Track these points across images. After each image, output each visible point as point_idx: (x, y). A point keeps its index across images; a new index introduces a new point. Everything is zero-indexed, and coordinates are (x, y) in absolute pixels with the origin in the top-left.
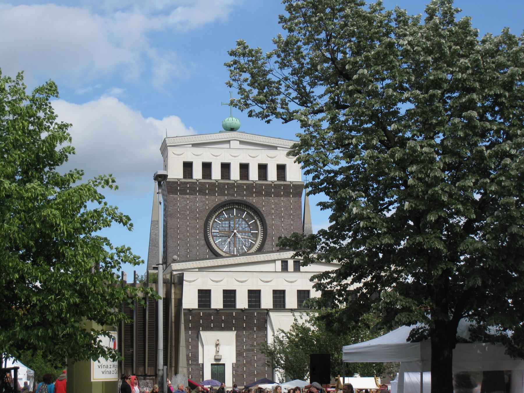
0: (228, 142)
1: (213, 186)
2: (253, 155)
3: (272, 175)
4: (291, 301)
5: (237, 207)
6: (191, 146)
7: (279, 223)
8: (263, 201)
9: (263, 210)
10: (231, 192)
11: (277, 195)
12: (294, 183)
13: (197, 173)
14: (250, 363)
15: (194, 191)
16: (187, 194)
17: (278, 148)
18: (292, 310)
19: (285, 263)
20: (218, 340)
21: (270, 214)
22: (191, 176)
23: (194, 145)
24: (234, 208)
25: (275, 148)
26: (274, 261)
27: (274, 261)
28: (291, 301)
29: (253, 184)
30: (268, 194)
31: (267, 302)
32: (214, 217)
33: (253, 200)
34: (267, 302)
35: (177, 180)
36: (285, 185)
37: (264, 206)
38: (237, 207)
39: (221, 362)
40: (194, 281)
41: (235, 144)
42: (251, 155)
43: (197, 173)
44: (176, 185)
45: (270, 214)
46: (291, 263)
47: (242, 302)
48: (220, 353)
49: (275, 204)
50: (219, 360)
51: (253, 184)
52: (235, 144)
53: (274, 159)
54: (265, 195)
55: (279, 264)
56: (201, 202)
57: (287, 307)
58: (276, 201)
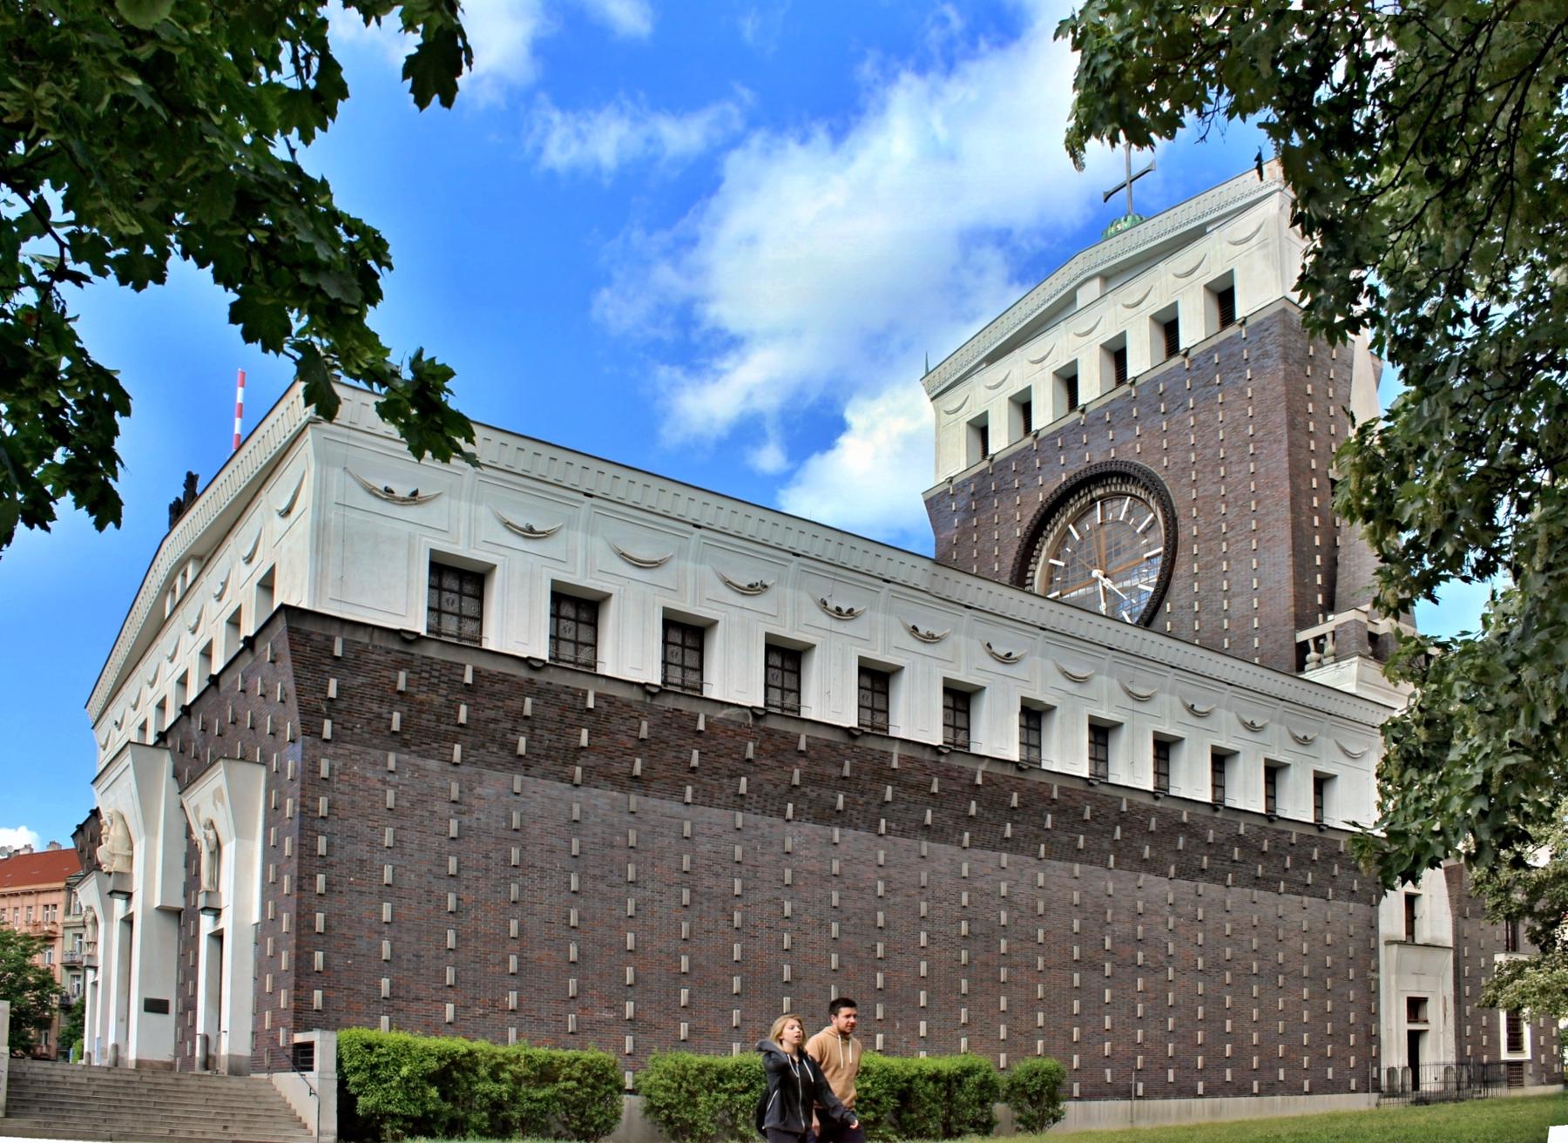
9: (1159, 466)
33: (1129, 448)
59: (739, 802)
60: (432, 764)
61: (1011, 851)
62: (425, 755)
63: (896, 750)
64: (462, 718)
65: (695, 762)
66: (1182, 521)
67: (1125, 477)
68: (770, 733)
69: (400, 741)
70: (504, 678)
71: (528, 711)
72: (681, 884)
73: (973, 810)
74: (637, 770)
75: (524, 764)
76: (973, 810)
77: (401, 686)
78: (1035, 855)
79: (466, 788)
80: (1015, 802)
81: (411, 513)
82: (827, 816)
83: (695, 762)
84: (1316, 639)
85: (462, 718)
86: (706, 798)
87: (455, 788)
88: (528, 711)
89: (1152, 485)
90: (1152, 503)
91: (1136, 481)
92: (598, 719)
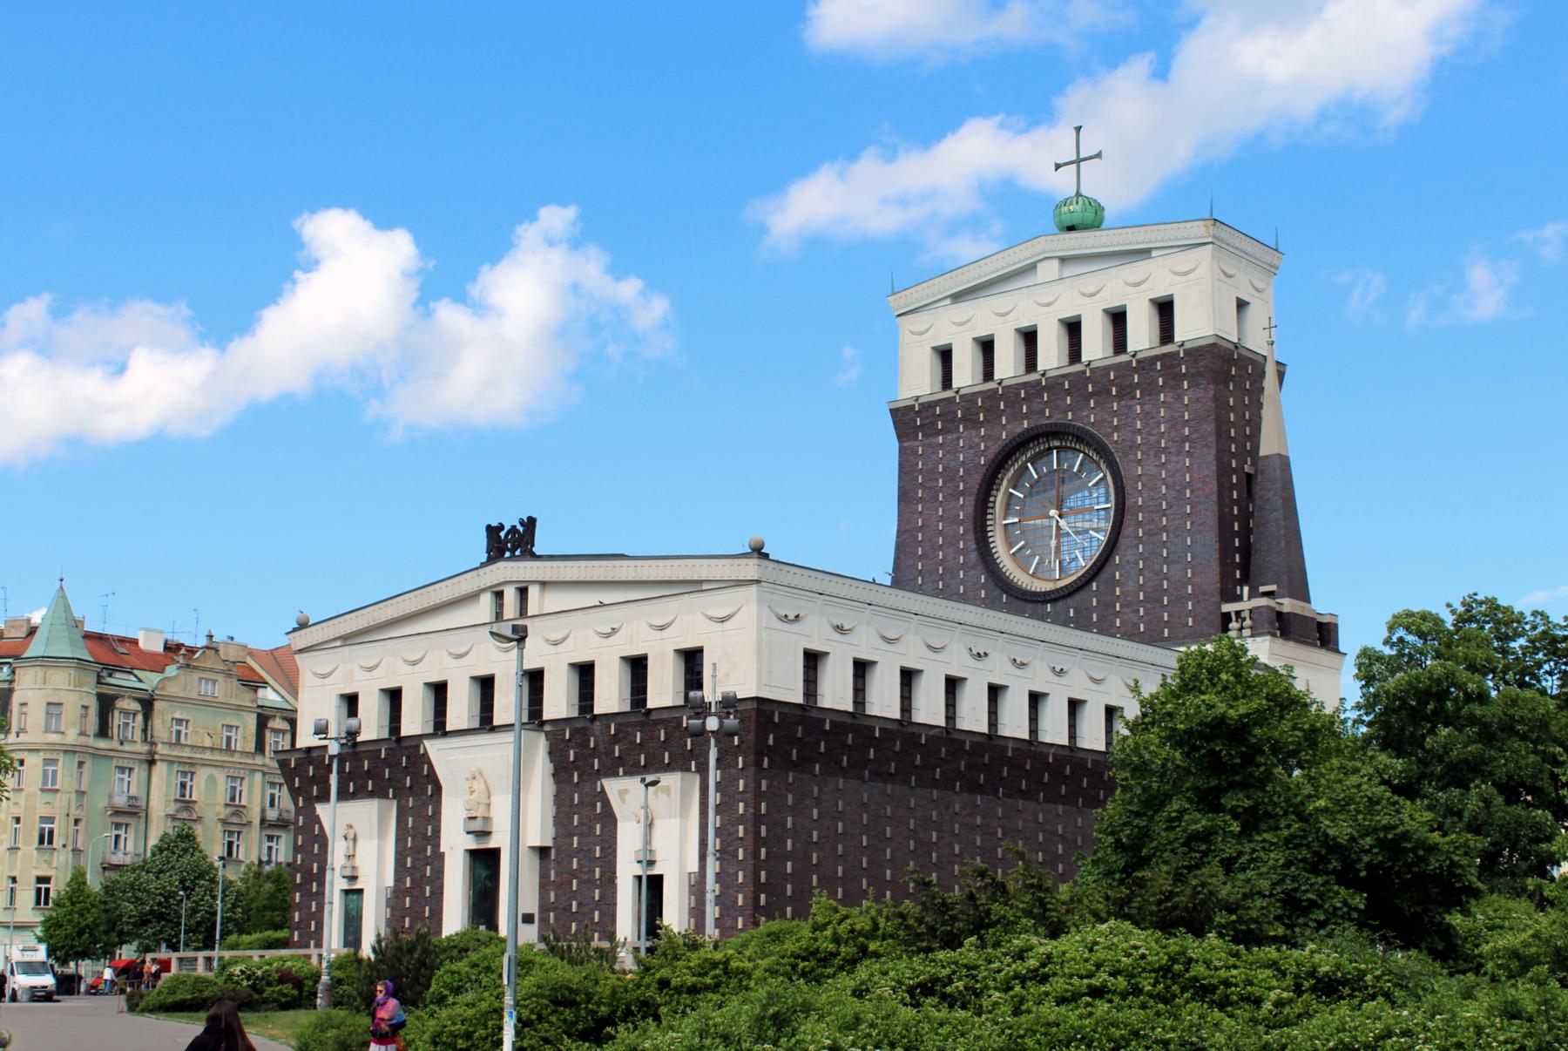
0: (1032, 268)
1: (990, 396)
2: (1092, 290)
3: (1142, 335)
4: (507, 705)
5: (1057, 443)
6: (948, 301)
7: (1155, 471)
8: (1115, 414)
10: (1036, 406)
11: (1150, 389)
12: (1187, 346)
13: (966, 374)
14: (418, 884)
15: (952, 421)
16: (939, 432)
17: (1154, 254)
18: (507, 727)
19: (499, 595)
20: (350, 827)
21: (1133, 447)
22: (947, 381)
23: (957, 297)
24: (1050, 449)
25: (1145, 253)
26: (473, 597)
27: (473, 597)
28: (507, 705)
29: (1084, 372)
30: (1126, 393)
31: (461, 710)
32: (1005, 483)
33: (1089, 419)
34: (461, 710)
35: (911, 402)
36: (1164, 355)
37: (1117, 428)
38: (1057, 443)
39: (357, 886)
40: (330, 674)
41: (1048, 270)
42: (1084, 291)
43: (966, 374)
44: (912, 415)
45: (1133, 447)
46: (510, 595)
47: (414, 721)
48: (358, 862)
49: (1146, 416)
50: (353, 878)
51: (1084, 372)
52: (1048, 270)
53: (1143, 287)
54: (1119, 397)
55: (487, 600)
56: (971, 447)
57: (496, 723)
58: (1147, 408)
59: (935, 784)
60: (806, 777)
61: (1063, 803)
62: (803, 772)
63: (1010, 745)
64: (822, 749)
65: (918, 762)
66: (1128, 490)
67: (1080, 439)
68: (953, 740)
69: (794, 766)
70: (842, 724)
71: (850, 741)
72: (909, 838)
73: (1046, 778)
74: (893, 770)
75: (843, 772)
76: (1046, 778)
77: (799, 734)
78: (1076, 805)
79: (820, 790)
80: (1068, 771)
81: (795, 627)
82: (973, 788)
83: (918, 762)
84: (1238, 613)
85: (822, 749)
86: (921, 782)
87: (816, 789)
88: (850, 741)
89: (1104, 452)
90: (1103, 466)
91: (1089, 445)
92: (878, 744)
